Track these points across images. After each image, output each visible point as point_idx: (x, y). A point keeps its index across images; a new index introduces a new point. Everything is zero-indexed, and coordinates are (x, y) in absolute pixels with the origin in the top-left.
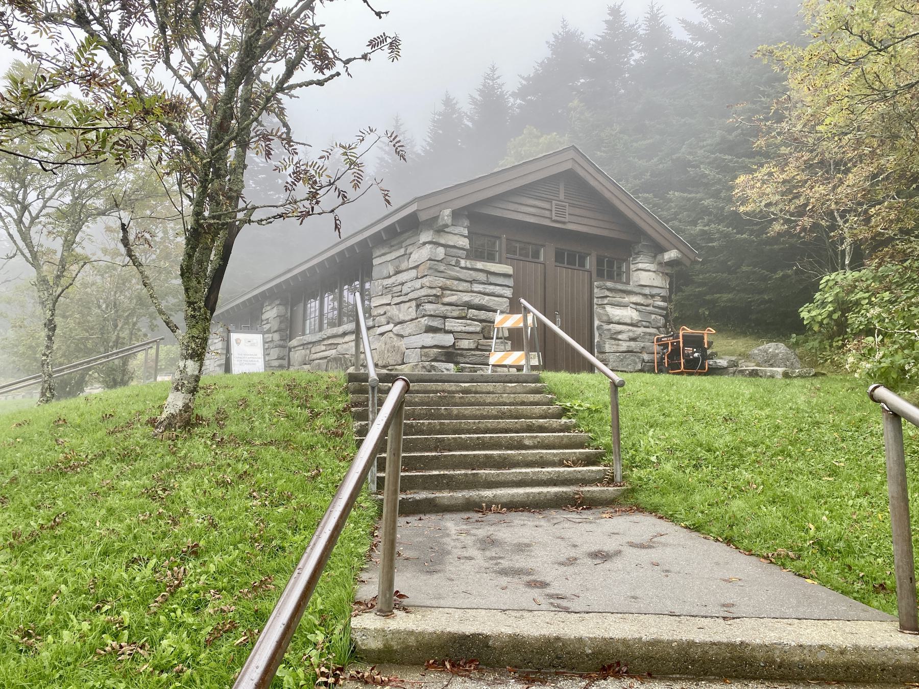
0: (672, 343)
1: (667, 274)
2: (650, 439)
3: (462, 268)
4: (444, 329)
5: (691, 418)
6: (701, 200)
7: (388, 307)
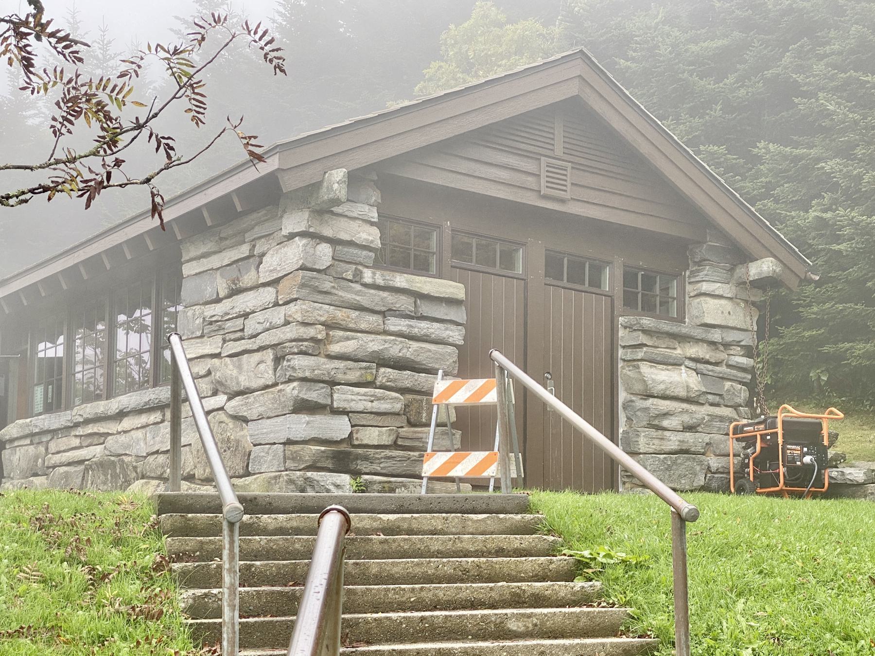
0: (763, 437)
1: (754, 304)
2: (739, 617)
3: (365, 285)
4: (331, 406)
5: (811, 578)
6: (818, 160)
7: (216, 361)
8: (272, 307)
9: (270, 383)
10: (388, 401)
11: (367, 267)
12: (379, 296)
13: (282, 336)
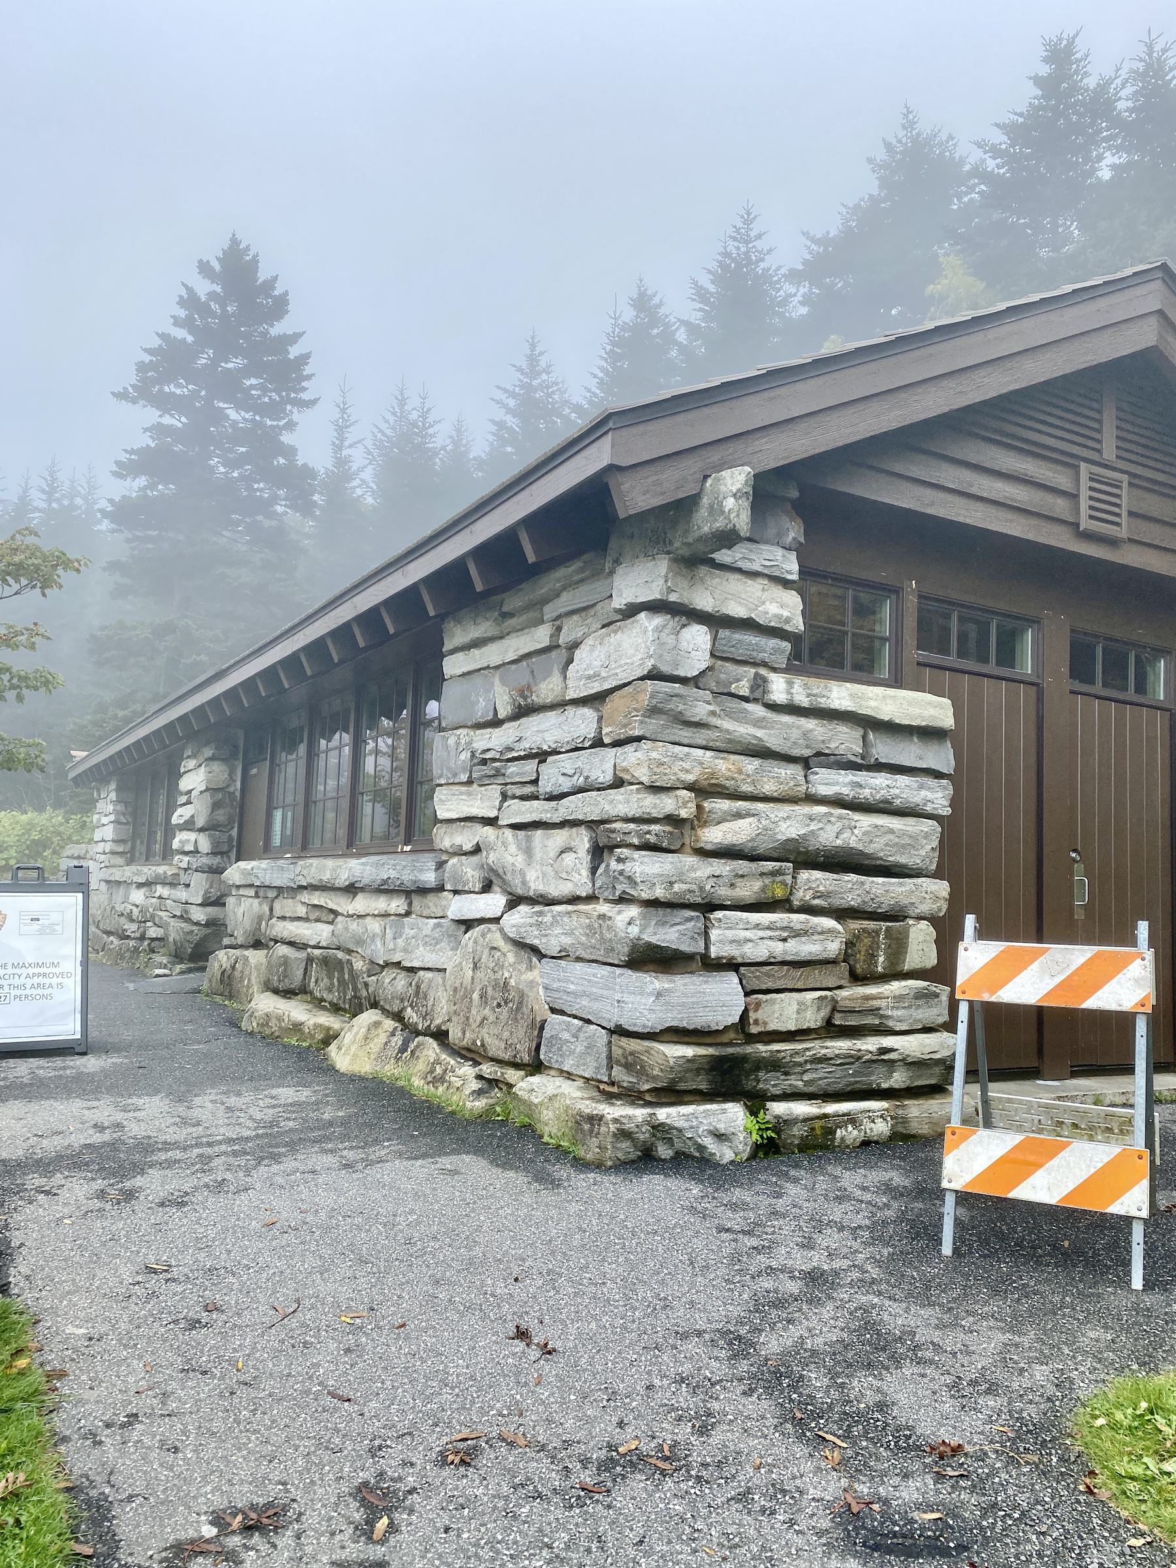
3: (774, 707)
8: (591, 747)
9: (584, 894)
10: (816, 937)
11: (775, 670)
12: (798, 727)
13: (607, 808)
